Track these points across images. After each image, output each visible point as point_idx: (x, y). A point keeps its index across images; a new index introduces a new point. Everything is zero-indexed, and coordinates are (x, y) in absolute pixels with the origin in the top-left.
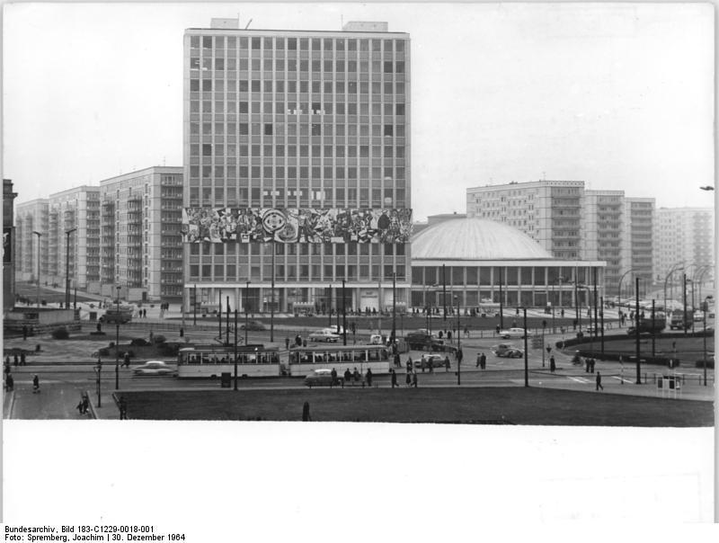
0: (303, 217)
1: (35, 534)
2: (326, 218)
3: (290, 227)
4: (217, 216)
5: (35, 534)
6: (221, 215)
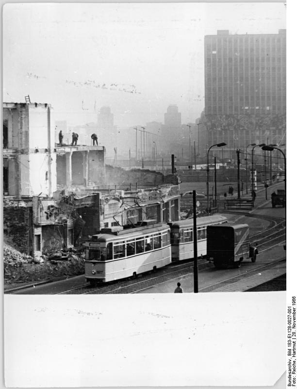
0: (257, 118)
1: (292, 370)
2: (268, 119)
3: (251, 123)
4: (220, 119)
5: (292, 370)
6: (221, 118)
